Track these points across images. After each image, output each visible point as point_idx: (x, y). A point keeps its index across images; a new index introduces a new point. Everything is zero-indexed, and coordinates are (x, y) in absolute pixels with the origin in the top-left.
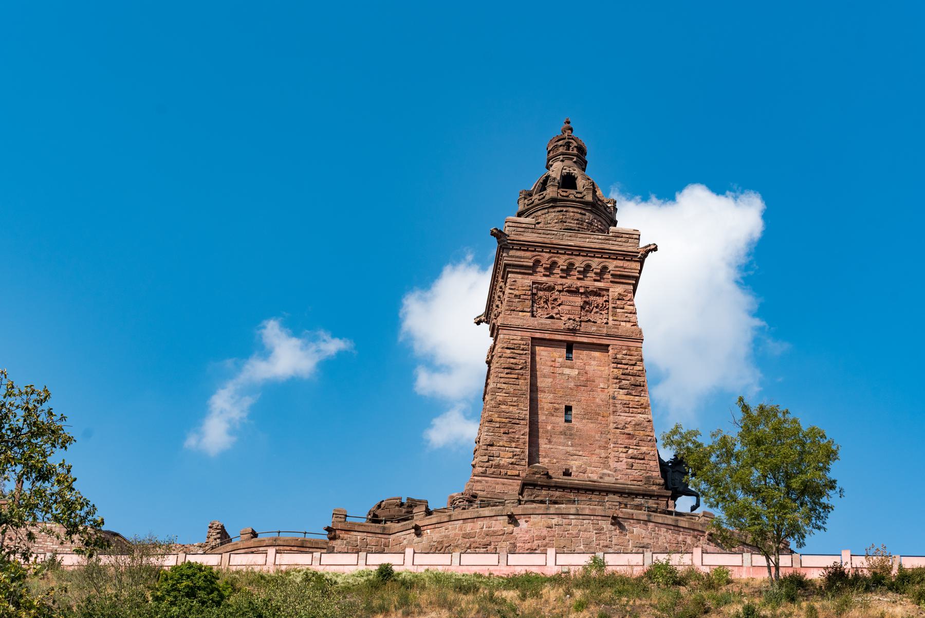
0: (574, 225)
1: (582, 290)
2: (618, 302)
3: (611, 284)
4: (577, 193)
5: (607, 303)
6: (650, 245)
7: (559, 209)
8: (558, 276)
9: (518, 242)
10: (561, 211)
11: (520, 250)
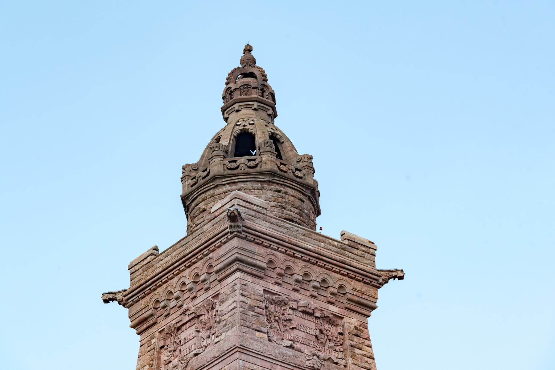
0: (293, 215)
1: (318, 314)
2: (356, 339)
3: (346, 312)
4: (282, 164)
5: (342, 337)
6: (396, 271)
7: (277, 187)
8: (290, 287)
9: (253, 232)
10: (279, 191)
11: (253, 241)
